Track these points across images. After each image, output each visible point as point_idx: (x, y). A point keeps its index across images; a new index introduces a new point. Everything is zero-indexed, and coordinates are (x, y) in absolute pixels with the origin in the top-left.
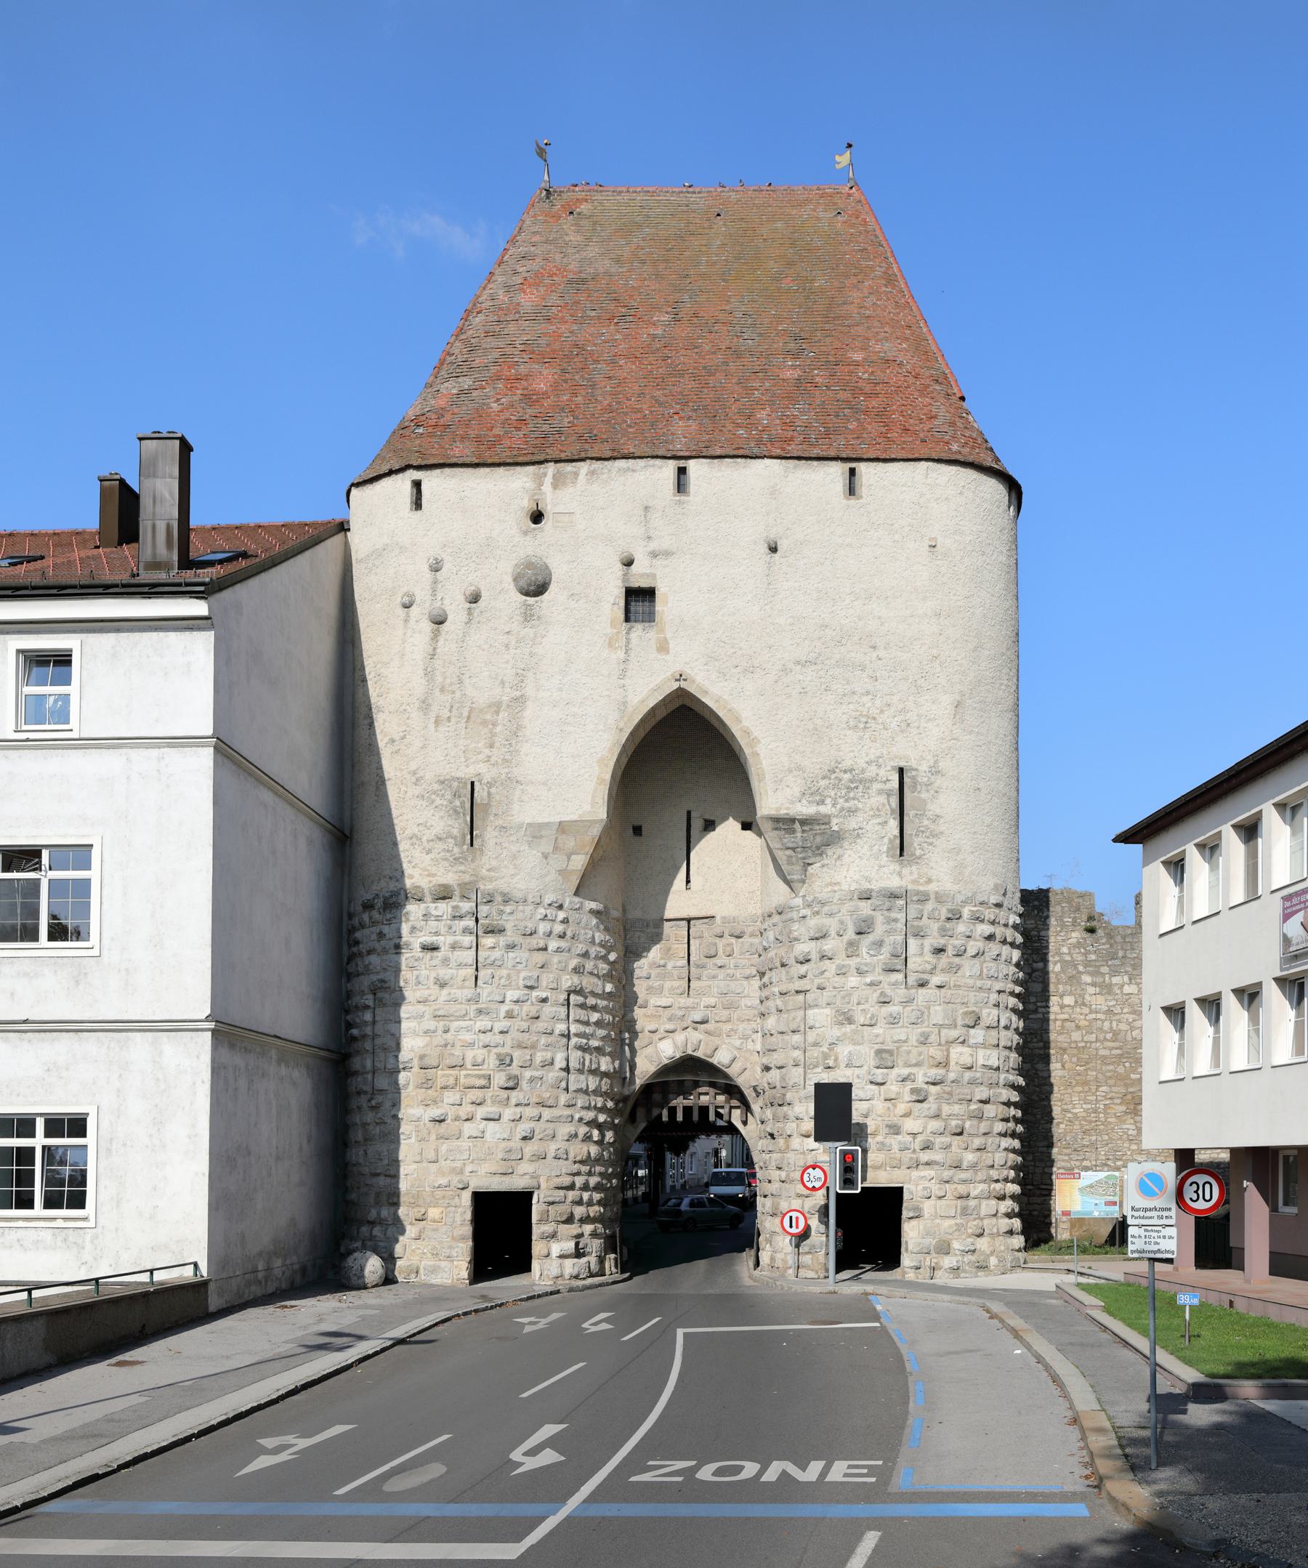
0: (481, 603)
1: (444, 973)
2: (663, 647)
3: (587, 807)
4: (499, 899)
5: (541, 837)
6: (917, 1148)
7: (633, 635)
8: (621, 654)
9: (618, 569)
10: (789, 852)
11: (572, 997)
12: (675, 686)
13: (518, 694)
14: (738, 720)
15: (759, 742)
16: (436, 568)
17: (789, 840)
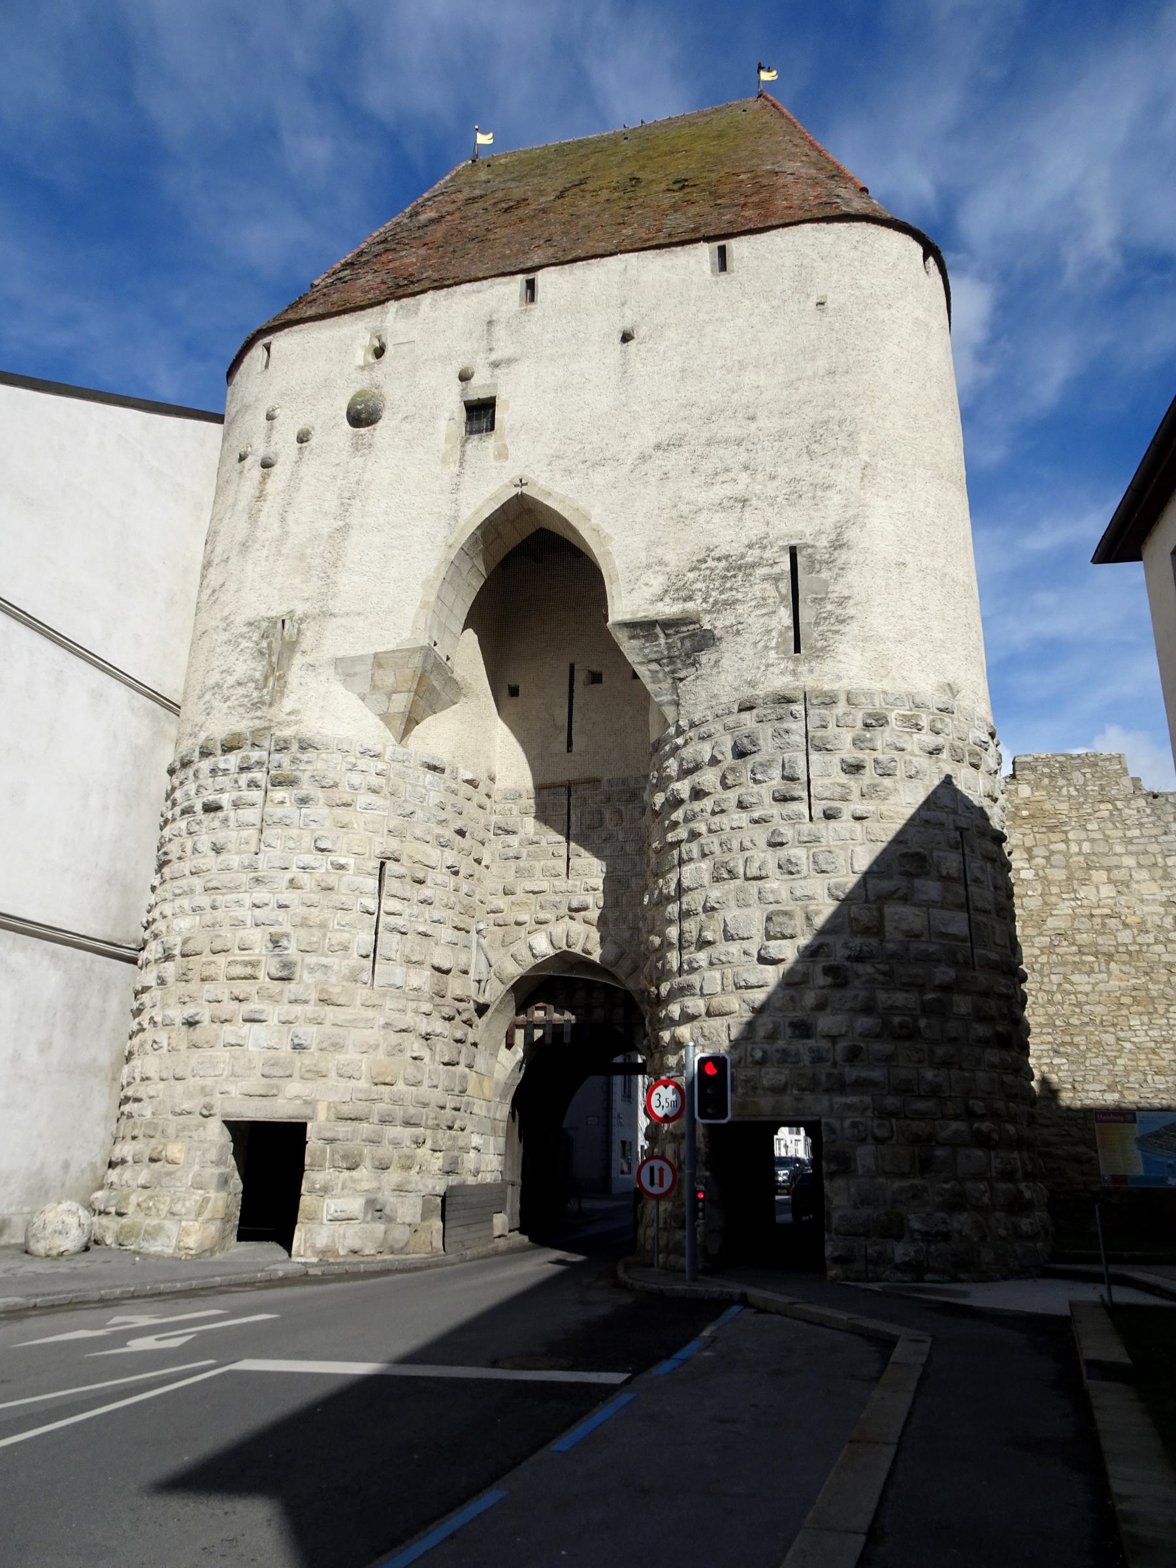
0: (313, 442)
1: (220, 836)
2: (502, 454)
3: (406, 634)
4: (295, 747)
5: (355, 674)
6: (839, 1058)
7: (469, 446)
8: (455, 468)
9: (457, 385)
10: (654, 666)
11: (390, 865)
12: (515, 491)
13: (341, 523)
14: (587, 519)
15: (611, 538)
16: (270, 417)
17: (650, 650)
